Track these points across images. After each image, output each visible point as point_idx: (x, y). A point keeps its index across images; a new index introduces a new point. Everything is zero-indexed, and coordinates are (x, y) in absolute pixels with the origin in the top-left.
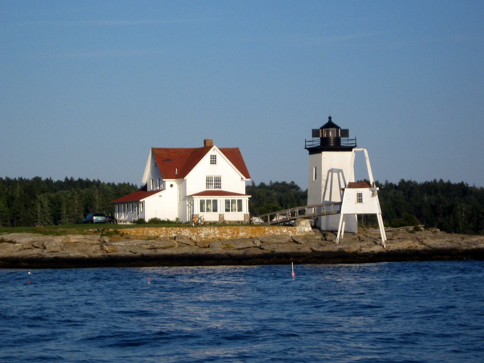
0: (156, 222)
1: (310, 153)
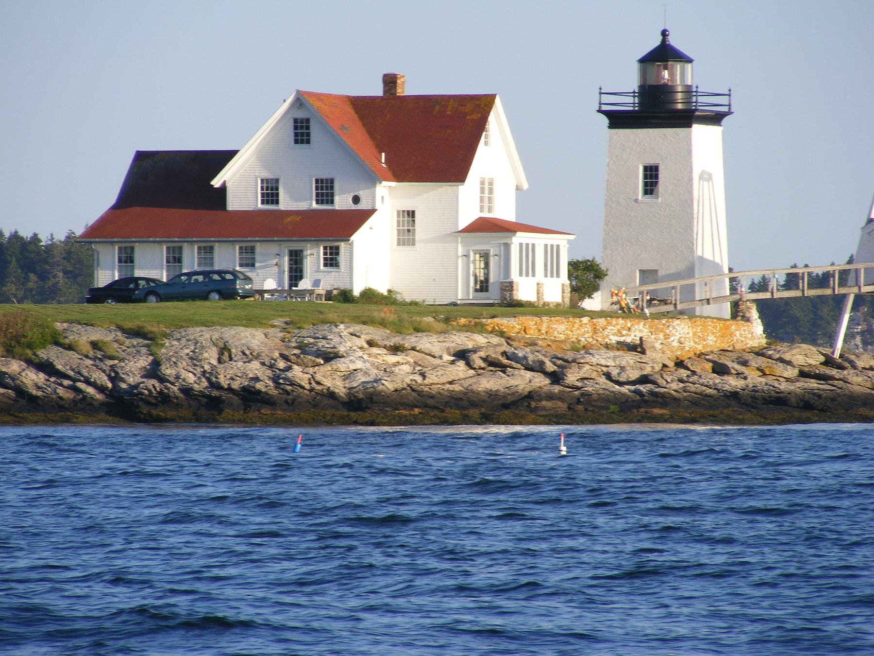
0: (369, 296)
1: (612, 126)
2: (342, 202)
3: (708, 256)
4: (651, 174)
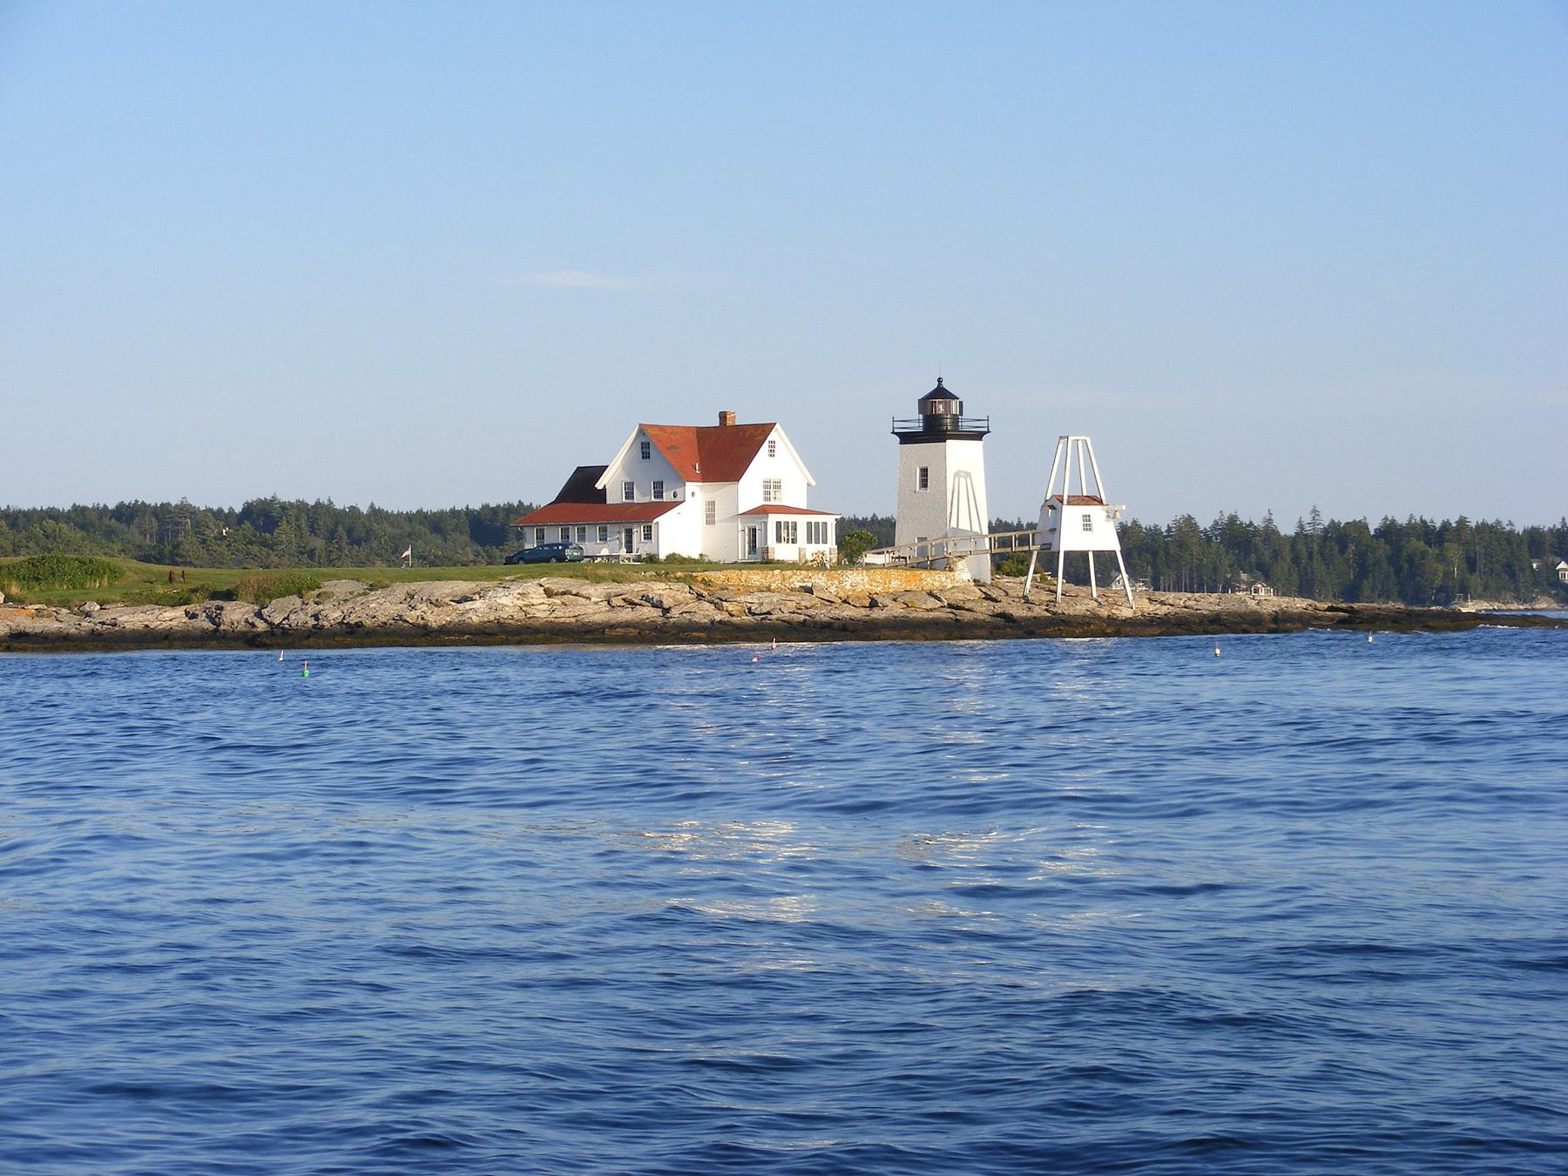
2: (667, 496)
3: (965, 525)
4: (924, 472)
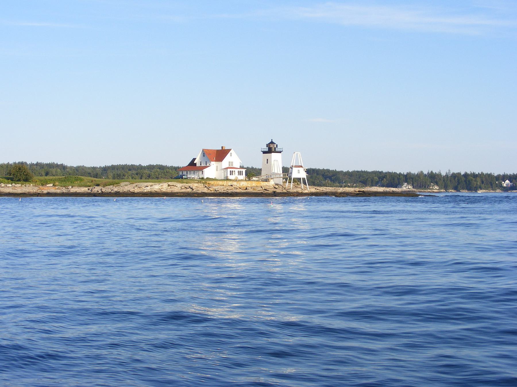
2: (208, 165)
3: (276, 172)
